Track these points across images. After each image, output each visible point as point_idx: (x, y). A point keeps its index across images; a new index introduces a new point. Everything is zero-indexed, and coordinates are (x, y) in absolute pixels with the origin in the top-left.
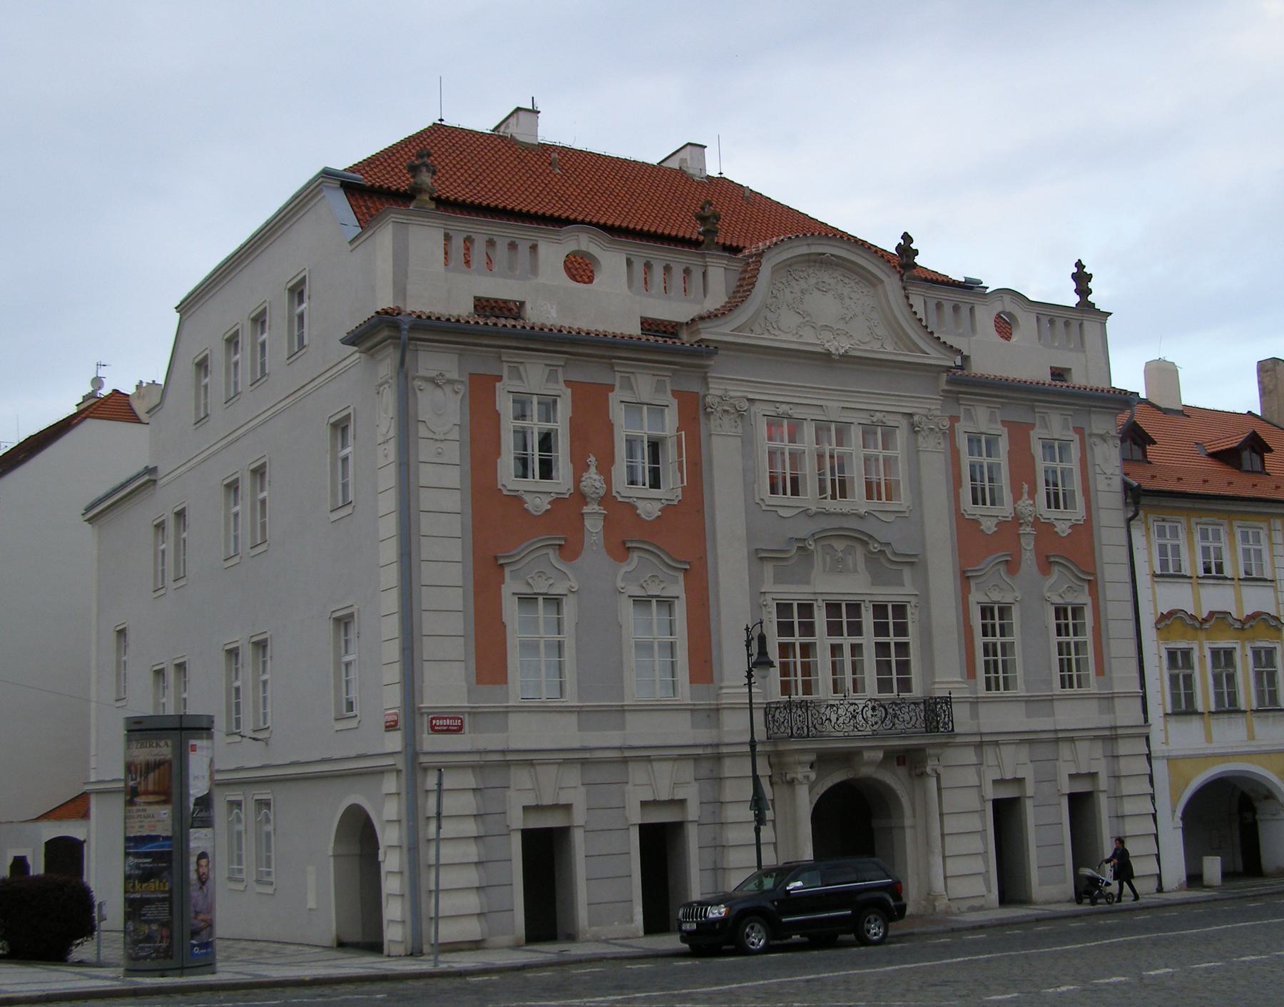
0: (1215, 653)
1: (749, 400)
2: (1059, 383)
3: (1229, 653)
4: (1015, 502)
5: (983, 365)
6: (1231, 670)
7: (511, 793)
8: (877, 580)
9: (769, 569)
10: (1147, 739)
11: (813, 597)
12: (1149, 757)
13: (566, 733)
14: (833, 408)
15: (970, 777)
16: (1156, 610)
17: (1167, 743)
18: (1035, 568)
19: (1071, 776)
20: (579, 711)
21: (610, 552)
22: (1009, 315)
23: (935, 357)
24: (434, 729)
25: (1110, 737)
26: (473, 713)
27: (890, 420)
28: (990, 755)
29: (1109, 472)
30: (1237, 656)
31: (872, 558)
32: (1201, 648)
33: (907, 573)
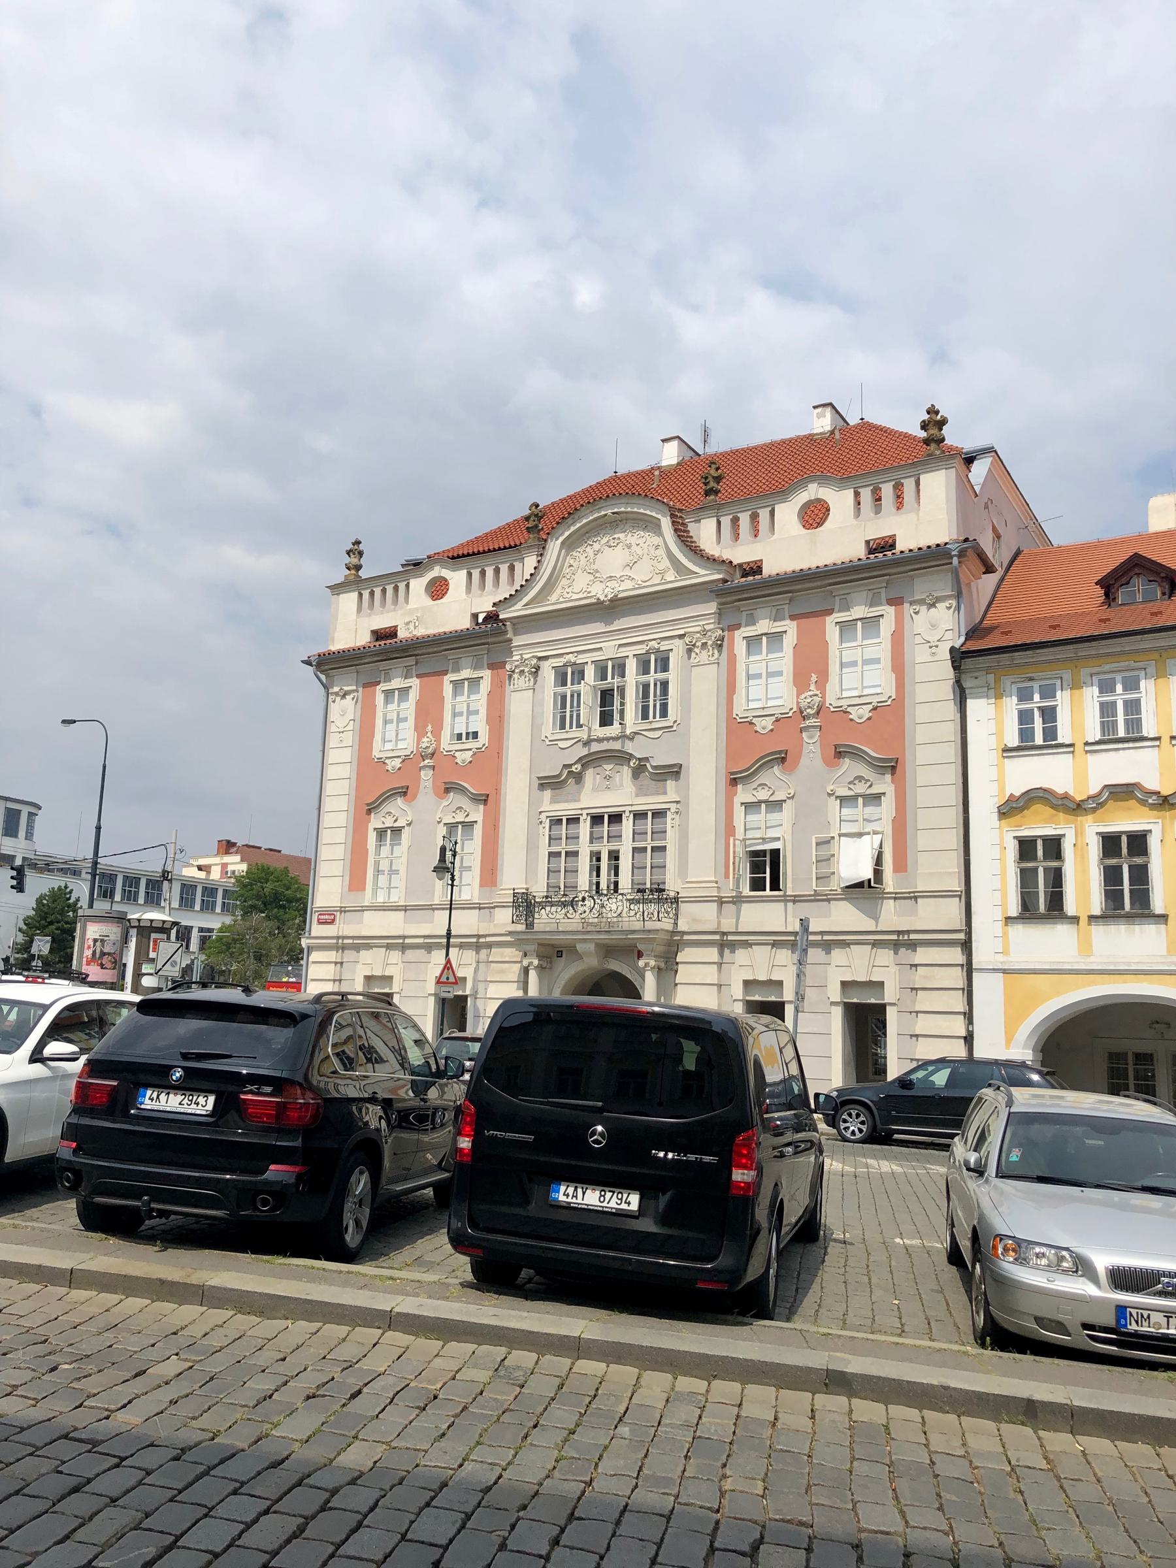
0: (1110, 843)
1: (540, 659)
2: (889, 553)
3: (1139, 842)
6: (1139, 860)
7: (359, 966)
8: (640, 792)
9: (548, 793)
10: (967, 946)
11: (580, 812)
14: (609, 649)
16: (1002, 788)
17: (1005, 952)
18: (819, 762)
20: (405, 909)
22: (819, 500)
24: (320, 922)
25: (902, 942)
26: (343, 910)
27: (664, 646)
28: (741, 955)
29: (933, 638)
30: (1154, 843)
31: (638, 771)
32: (1079, 833)
33: (670, 784)
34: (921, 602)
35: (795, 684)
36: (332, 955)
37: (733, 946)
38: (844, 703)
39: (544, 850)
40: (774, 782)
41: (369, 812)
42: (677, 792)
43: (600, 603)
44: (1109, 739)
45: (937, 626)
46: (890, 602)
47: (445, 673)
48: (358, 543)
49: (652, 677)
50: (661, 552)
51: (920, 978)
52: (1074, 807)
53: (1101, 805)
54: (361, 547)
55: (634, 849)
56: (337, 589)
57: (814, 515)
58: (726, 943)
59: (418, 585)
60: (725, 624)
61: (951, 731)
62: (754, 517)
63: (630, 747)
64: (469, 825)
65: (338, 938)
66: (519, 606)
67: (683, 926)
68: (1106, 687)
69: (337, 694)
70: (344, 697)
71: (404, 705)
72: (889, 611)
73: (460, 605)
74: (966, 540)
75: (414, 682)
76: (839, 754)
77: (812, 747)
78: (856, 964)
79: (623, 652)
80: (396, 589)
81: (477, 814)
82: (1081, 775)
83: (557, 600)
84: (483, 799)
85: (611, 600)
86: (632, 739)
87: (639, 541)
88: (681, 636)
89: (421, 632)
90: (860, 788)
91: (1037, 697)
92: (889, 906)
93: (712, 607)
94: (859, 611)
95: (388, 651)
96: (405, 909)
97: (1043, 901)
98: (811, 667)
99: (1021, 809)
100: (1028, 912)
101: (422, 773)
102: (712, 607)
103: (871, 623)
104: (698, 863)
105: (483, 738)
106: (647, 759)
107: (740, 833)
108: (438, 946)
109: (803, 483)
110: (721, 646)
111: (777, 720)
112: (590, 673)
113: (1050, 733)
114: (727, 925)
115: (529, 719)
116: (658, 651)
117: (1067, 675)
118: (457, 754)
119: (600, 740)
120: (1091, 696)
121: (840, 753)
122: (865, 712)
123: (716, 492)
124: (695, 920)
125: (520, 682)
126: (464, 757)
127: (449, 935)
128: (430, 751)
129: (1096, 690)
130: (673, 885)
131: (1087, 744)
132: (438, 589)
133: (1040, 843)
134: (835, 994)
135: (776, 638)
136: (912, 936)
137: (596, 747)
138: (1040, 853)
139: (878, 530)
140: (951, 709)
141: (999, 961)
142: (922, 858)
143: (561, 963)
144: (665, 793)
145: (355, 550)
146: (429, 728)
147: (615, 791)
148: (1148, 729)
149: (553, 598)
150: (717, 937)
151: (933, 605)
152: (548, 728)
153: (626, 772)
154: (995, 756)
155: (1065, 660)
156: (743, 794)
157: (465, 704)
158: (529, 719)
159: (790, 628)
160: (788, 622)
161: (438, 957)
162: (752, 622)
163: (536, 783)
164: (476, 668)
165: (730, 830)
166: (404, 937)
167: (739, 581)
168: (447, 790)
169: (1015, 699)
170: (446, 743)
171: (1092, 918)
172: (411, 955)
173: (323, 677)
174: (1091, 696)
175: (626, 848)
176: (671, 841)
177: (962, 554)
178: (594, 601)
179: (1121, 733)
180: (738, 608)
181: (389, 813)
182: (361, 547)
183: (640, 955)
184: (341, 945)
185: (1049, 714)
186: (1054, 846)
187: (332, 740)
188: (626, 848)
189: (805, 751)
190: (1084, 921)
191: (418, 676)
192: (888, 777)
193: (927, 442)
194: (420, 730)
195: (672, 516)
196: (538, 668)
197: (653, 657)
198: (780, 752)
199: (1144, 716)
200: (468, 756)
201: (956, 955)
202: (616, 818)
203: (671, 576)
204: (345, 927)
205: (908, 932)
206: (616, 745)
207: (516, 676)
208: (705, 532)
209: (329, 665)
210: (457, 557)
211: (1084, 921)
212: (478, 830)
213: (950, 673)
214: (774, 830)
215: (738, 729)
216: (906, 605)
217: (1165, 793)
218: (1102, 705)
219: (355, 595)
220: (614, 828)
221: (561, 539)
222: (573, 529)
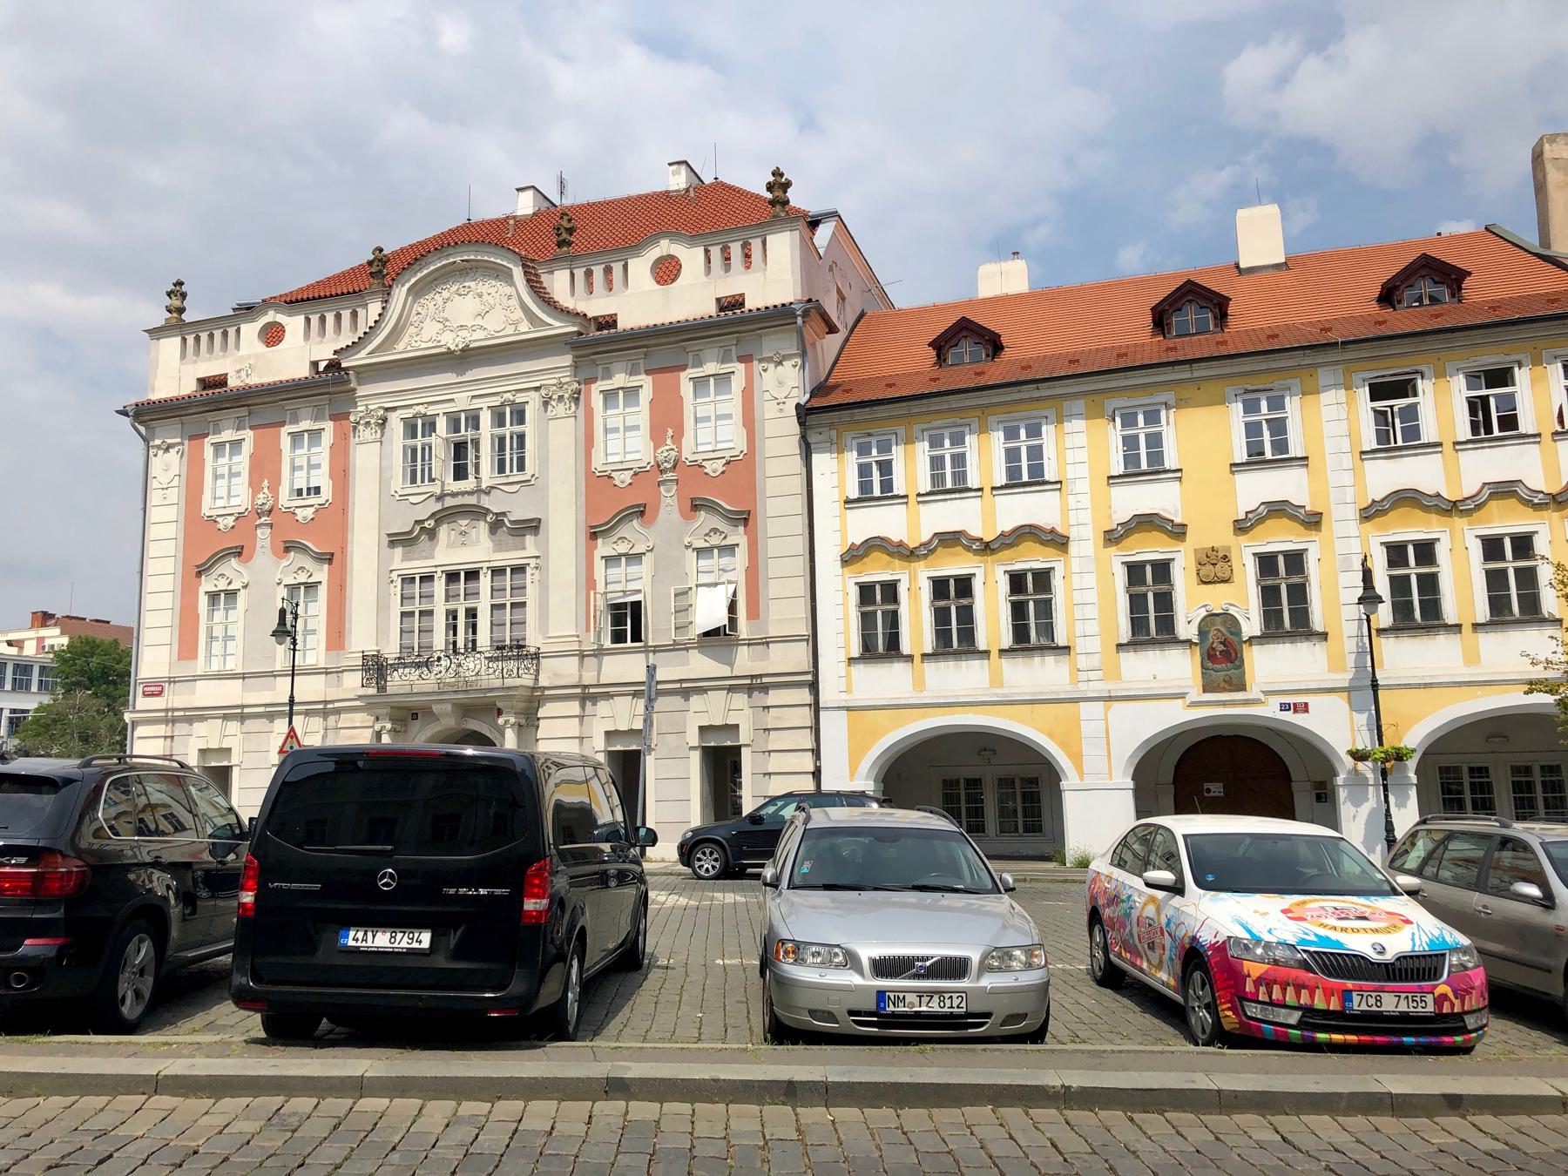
0: (939, 587)
1: (387, 409)
4: (656, 449)
5: (628, 321)
6: (964, 602)
7: (192, 740)
8: (499, 547)
9: (399, 551)
10: (814, 686)
12: (816, 707)
13: (231, 693)
14: (462, 401)
15: (573, 728)
17: (848, 691)
18: (676, 515)
19: (701, 728)
20: (243, 677)
21: (274, 553)
22: (671, 257)
23: (559, 327)
24: (145, 695)
25: (755, 686)
26: (172, 681)
27: (520, 398)
28: (603, 707)
29: (781, 396)
30: (977, 586)
31: (496, 526)
33: (529, 539)
34: (769, 360)
35: (652, 438)
36: (161, 729)
37: (594, 698)
38: (699, 457)
39: (396, 609)
40: (634, 535)
41: (199, 574)
42: (537, 546)
43: (450, 352)
44: (938, 490)
45: (784, 383)
46: (741, 359)
47: (282, 424)
48: (180, 284)
49: (508, 430)
50: (514, 302)
51: (771, 719)
52: (908, 554)
53: (932, 551)
54: (184, 288)
55: (493, 606)
56: (156, 333)
57: (667, 271)
58: (587, 696)
59: (250, 330)
60: (582, 376)
61: (798, 484)
62: (608, 271)
63: (486, 502)
64: (311, 587)
65: (167, 710)
66: (363, 353)
67: (543, 682)
68: (936, 443)
69: (159, 447)
70: (167, 450)
71: (236, 459)
72: (739, 368)
73: (299, 351)
74: (810, 300)
75: (248, 435)
76: (695, 507)
77: (669, 502)
78: (713, 709)
79: (477, 404)
80: (225, 334)
81: (321, 574)
82: (914, 523)
83: (405, 348)
84: (328, 558)
85: (463, 350)
86: (488, 493)
87: (492, 290)
88: (537, 389)
89: (254, 380)
90: (715, 540)
91: (874, 452)
92: (743, 651)
93: (567, 360)
94: (711, 368)
95: (216, 400)
96: (243, 677)
97: (880, 642)
98: (667, 422)
99: (861, 557)
100: (869, 653)
101: (259, 531)
102: (567, 360)
103: (723, 379)
104: (558, 616)
105: (327, 494)
106: (504, 514)
107: (600, 587)
108: (280, 714)
109: (654, 239)
110: (577, 399)
111: (636, 474)
112: (442, 424)
113: (887, 485)
114: (589, 678)
115: (377, 476)
116: (513, 403)
117: (901, 431)
118: (298, 511)
119: (454, 495)
120: (922, 450)
121: (696, 506)
122: (719, 466)
123: (569, 244)
124: (556, 675)
125: (366, 434)
126: (304, 514)
127: (292, 702)
128: (267, 507)
129: (926, 444)
130: (533, 641)
131: (919, 495)
132: (273, 335)
133: (878, 587)
134: (693, 739)
135: (632, 392)
136: (765, 680)
137: (449, 502)
138: (878, 597)
139: (728, 288)
140: (797, 464)
141: (844, 700)
142: (773, 606)
143: (416, 725)
144: (524, 548)
145: (178, 291)
146: (266, 483)
147: (472, 547)
148: (972, 482)
149: (400, 346)
150: (579, 691)
151: (780, 363)
152: (398, 482)
153: (483, 527)
154: (838, 506)
155: (901, 416)
156: (603, 548)
157: (305, 459)
158: (377, 476)
159: (646, 382)
160: (643, 376)
161: (281, 726)
162: (608, 375)
163: (386, 540)
164: (316, 419)
165: (591, 583)
166: (243, 707)
167: (595, 334)
168: (287, 550)
169: (855, 453)
170: (285, 499)
171: (924, 656)
172: (251, 725)
173: (142, 429)
174: (922, 450)
175: (484, 606)
176: (531, 596)
177: (806, 314)
178: (443, 350)
179: (949, 485)
180: (594, 361)
181: (222, 575)
182: (184, 288)
183: (500, 712)
184: (170, 718)
185: (886, 468)
186: (890, 590)
187: (155, 498)
188: (484, 606)
189: (663, 505)
190: (917, 659)
191: (252, 428)
192: (741, 529)
193: (772, 203)
194: (255, 486)
195: (524, 266)
196: (383, 422)
197: (508, 410)
198: (638, 506)
199: (968, 469)
200: (309, 513)
201: (805, 696)
202: (473, 575)
203: (524, 326)
204: (176, 698)
205: (761, 676)
206: (472, 500)
207: (361, 428)
208: (558, 283)
209: (149, 415)
210: (293, 302)
211: (917, 659)
212: (323, 591)
213: (796, 429)
214: (635, 582)
215: (596, 483)
216: (755, 363)
217: (987, 539)
218: (932, 458)
219: (178, 340)
220: (471, 585)
221: (407, 286)
222: (420, 275)
